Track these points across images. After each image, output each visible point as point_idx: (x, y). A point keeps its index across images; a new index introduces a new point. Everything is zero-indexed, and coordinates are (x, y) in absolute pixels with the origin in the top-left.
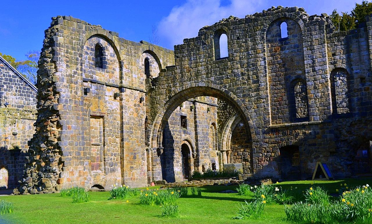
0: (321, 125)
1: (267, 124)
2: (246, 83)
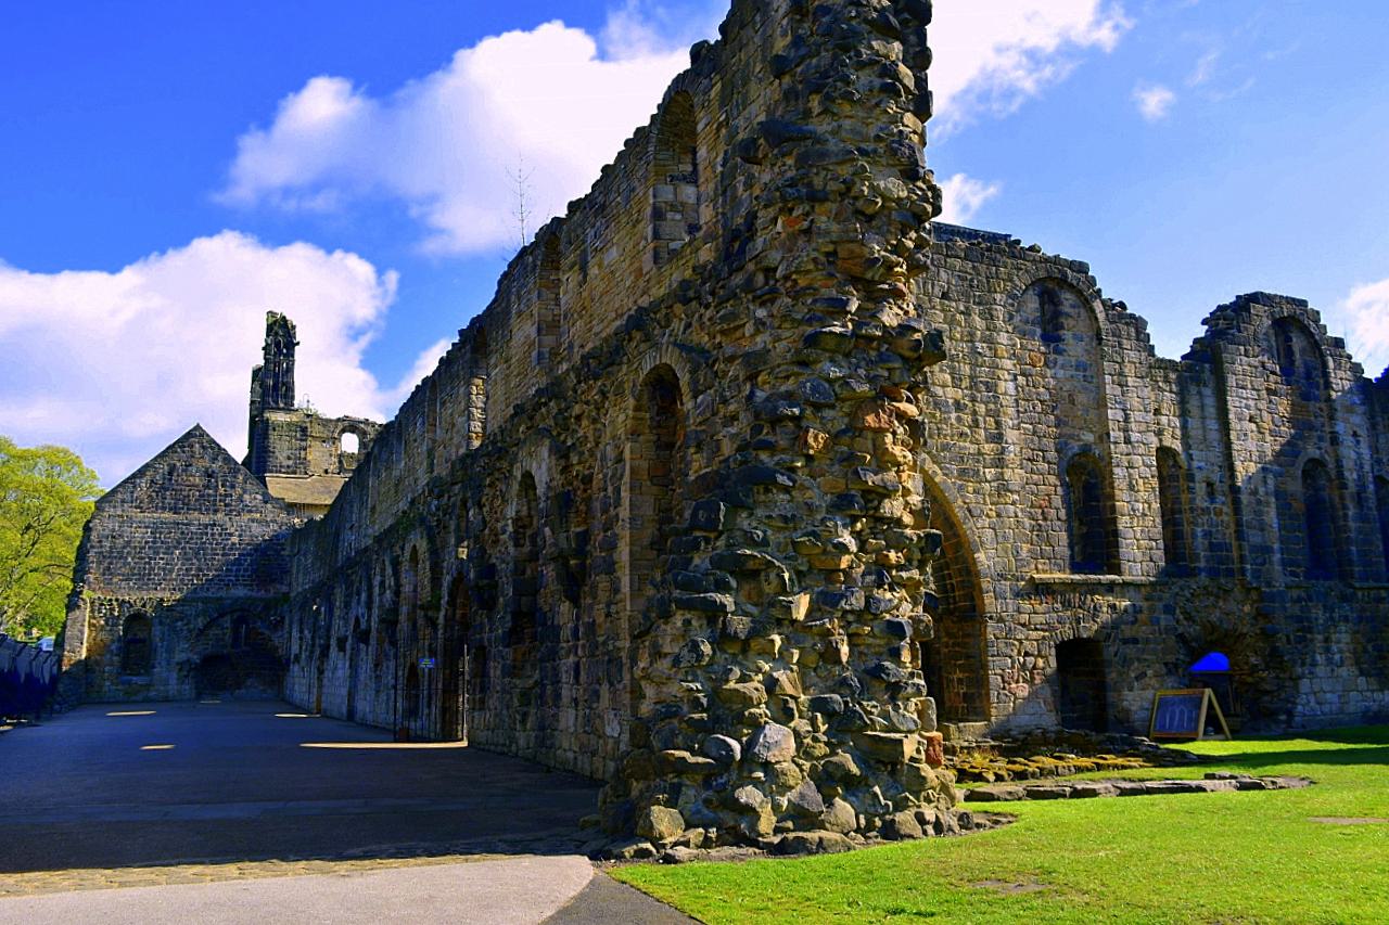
0: (1148, 589)
1: (1024, 570)
2: (966, 434)
